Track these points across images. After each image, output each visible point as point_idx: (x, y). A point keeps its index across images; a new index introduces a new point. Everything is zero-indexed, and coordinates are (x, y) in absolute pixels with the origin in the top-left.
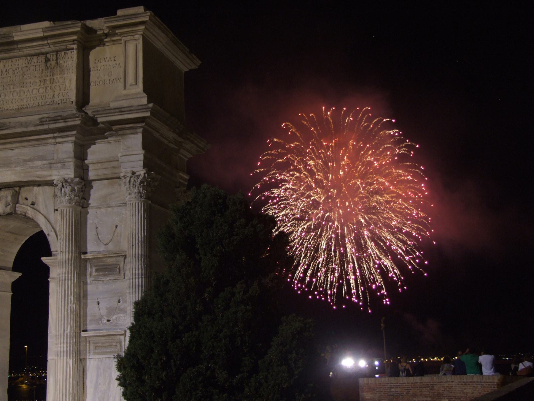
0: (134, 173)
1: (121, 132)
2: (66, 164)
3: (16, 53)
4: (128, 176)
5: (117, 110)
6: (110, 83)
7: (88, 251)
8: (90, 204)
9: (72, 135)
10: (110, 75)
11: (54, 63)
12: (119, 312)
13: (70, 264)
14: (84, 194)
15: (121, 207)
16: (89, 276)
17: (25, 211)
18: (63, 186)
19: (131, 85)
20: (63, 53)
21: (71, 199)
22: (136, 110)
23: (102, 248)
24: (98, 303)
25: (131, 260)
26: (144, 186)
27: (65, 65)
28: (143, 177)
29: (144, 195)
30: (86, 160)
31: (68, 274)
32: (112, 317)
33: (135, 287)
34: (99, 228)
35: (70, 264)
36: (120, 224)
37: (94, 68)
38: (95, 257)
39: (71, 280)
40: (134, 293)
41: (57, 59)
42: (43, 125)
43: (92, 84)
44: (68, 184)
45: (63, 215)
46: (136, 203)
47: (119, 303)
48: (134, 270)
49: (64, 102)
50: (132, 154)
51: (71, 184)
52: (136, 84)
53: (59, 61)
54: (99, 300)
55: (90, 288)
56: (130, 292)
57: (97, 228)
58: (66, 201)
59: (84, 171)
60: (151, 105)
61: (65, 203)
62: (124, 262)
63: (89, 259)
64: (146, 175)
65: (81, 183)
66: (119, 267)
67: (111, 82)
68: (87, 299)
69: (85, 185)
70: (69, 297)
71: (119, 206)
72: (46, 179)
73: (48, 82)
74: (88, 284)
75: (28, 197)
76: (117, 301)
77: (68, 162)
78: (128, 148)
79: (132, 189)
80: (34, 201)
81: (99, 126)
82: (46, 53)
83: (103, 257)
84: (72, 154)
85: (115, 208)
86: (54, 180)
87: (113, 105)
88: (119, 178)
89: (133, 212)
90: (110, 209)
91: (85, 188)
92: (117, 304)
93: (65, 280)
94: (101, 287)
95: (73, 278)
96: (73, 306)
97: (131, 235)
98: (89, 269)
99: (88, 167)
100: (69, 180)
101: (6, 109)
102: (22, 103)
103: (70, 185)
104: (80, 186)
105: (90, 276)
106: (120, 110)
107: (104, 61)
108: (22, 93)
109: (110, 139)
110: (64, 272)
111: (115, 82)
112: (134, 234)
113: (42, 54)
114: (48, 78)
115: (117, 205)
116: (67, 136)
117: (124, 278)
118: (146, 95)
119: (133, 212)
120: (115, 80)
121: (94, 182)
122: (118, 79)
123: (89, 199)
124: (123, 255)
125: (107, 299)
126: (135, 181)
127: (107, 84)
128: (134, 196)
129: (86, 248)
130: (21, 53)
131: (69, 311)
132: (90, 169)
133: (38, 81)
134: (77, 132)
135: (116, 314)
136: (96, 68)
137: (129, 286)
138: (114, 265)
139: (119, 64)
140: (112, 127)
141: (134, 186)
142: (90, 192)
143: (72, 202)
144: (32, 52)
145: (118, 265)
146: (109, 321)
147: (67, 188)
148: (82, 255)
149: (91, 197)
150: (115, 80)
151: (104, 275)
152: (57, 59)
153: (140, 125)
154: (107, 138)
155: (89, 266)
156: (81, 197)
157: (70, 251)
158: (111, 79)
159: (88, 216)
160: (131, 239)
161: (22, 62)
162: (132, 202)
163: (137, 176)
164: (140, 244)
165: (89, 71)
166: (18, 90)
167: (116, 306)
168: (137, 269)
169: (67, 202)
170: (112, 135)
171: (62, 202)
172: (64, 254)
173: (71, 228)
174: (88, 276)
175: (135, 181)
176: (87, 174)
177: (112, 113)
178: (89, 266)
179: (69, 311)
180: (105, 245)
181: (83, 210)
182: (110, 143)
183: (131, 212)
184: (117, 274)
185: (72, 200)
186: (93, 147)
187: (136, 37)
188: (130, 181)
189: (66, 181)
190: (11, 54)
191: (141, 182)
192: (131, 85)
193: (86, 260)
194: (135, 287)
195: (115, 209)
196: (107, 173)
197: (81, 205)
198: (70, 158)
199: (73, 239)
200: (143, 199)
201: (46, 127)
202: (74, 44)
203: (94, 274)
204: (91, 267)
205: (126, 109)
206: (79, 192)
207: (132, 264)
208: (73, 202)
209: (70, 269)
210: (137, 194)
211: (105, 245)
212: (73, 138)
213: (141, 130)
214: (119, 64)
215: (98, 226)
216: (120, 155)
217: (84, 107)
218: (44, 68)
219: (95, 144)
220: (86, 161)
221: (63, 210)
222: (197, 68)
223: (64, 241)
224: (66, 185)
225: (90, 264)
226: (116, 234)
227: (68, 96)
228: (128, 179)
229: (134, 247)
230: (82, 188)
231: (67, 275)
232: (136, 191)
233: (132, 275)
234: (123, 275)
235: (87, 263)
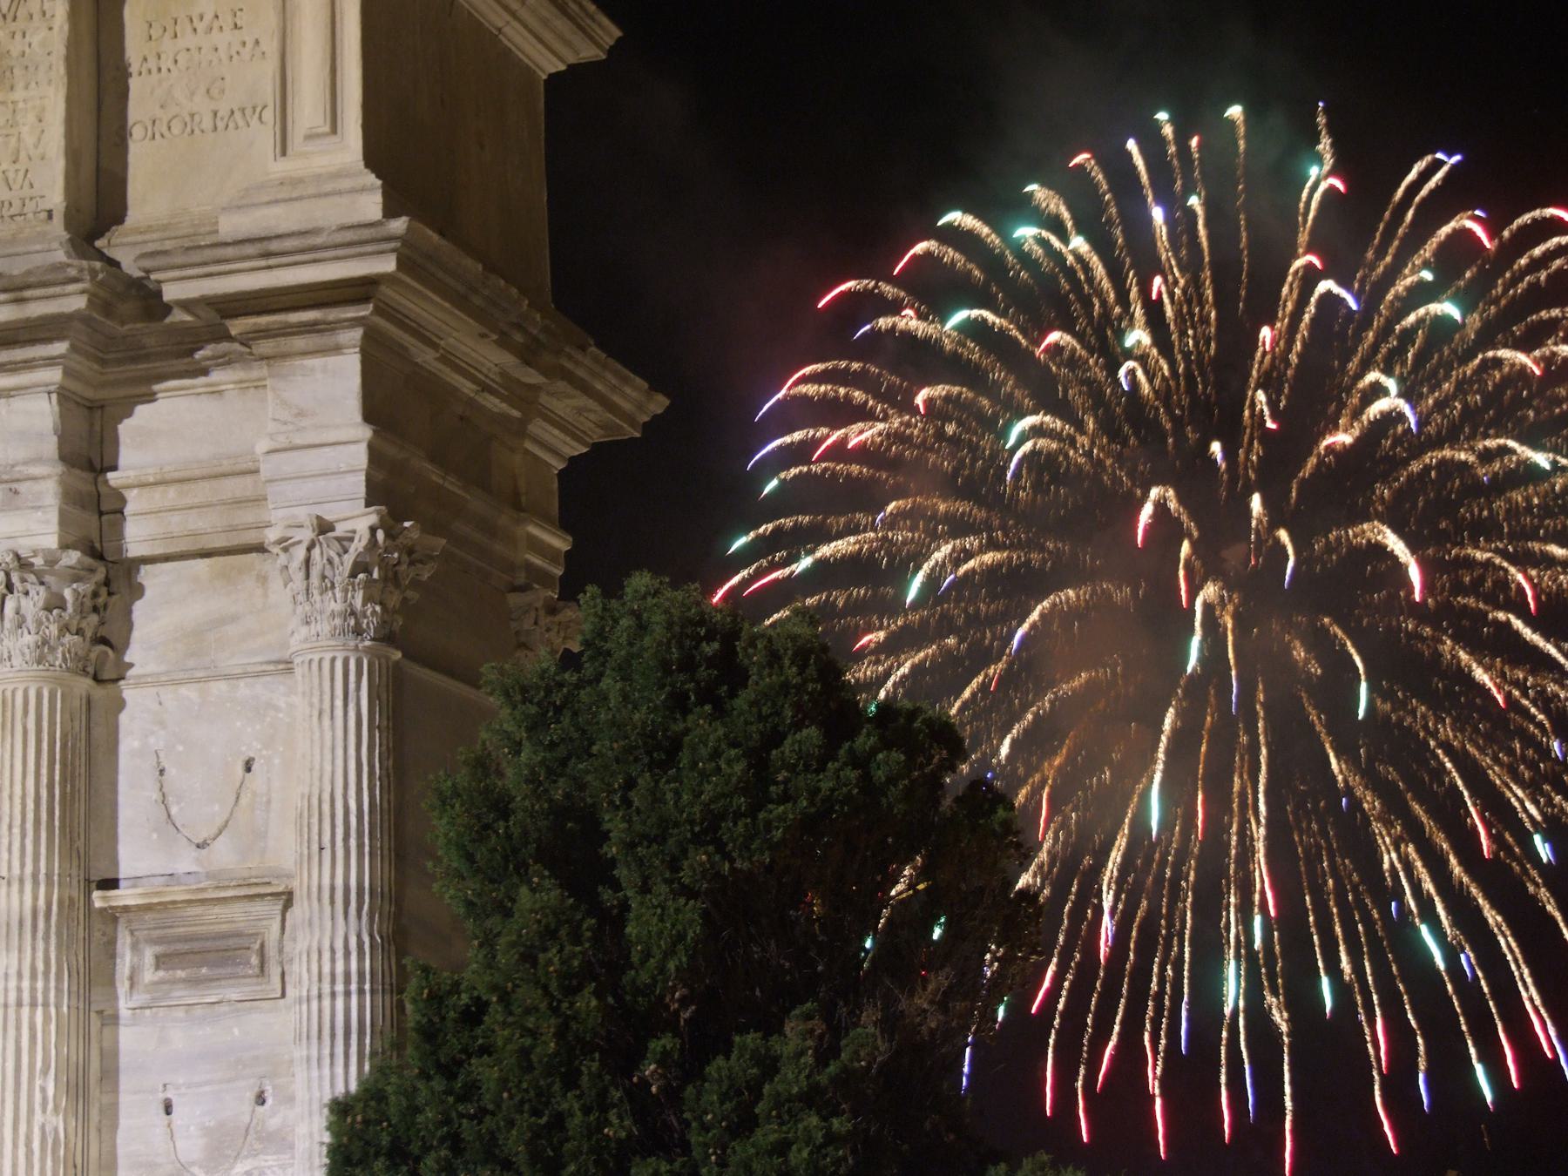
0: (324, 527)
1: (265, 347)
2: (23, 487)
4: (300, 542)
5: (250, 249)
6: (215, 128)
7: (121, 876)
8: (131, 665)
9: (50, 361)
10: (215, 92)
12: (257, 1146)
13: (40, 934)
14: (102, 623)
15: (268, 678)
16: (127, 984)
18: (10, 587)
19: (310, 137)
21: (45, 642)
22: (336, 246)
23: (186, 862)
24: (168, 1109)
25: (311, 912)
26: (369, 584)
27: (15, 53)
28: (364, 541)
29: (370, 623)
30: (114, 468)
31: (34, 977)
32: (232, 1168)
33: (333, 1036)
34: (172, 772)
35: (40, 934)
36: (264, 752)
37: (145, 59)
38: (155, 900)
39: (46, 1005)
40: (327, 1061)
43: (137, 132)
44: (32, 578)
45: (9, 714)
46: (333, 660)
47: (260, 1109)
48: (326, 955)
49: (13, 211)
50: (317, 442)
51: (47, 578)
52: (334, 130)
54: (169, 1095)
55: (130, 1039)
56: (308, 1059)
57: (162, 772)
58: (23, 654)
59: (104, 518)
60: (399, 225)
61: (17, 661)
62: (283, 921)
63: (126, 909)
64: (380, 535)
65: (92, 571)
66: (262, 946)
67: (220, 125)
68: (115, 1090)
69: (107, 582)
70: (38, 1082)
71: (258, 675)
74: (122, 1022)
76: (250, 1095)
77: (34, 479)
78: (301, 414)
79: (317, 597)
81: (168, 320)
83: (189, 902)
84: (51, 446)
85: (242, 683)
87: (232, 225)
88: (260, 549)
89: (321, 701)
90: (220, 687)
91: (110, 594)
92: (253, 1111)
93: (19, 1004)
94: (182, 1036)
95: (57, 996)
96: (54, 1119)
97: (315, 802)
98: (128, 958)
99: (123, 501)
100: (38, 562)
103: (42, 583)
104: (85, 588)
105: (132, 986)
106: (265, 248)
107: (189, 29)
109: (216, 376)
110: (13, 971)
111: (241, 123)
112: (326, 797)
115: (249, 669)
116: (28, 365)
117: (283, 995)
118: (379, 182)
119: (321, 701)
120: (238, 115)
121: (148, 567)
122: (254, 109)
123: (126, 644)
124: (281, 889)
125: (207, 1088)
126: (330, 561)
127: (203, 131)
128: (324, 627)
129: (115, 862)
131: (36, 1145)
132: (127, 511)
134: (73, 348)
135: (246, 1157)
136: (152, 64)
137: (305, 1030)
138: (239, 935)
139: (257, 42)
140: (228, 323)
141: (328, 586)
142: (130, 612)
143: (50, 658)
145: (257, 934)
147: (27, 593)
148: (96, 894)
149: (136, 635)
150: (238, 115)
153: (351, 312)
154: (205, 372)
155: (124, 941)
156: (89, 634)
157: (42, 877)
158: (223, 112)
159: (124, 718)
160: (315, 820)
162: (316, 657)
163: (339, 539)
164: (353, 842)
165: (123, 74)
167: (247, 1119)
168: (340, 954)
169: (28, 658)
170: (226, 361)
171: (6, 656)
172: (15, 887)
173: (44, 771)
174: (122, 988)
175: (330, 561)
176: (120, 535)
177: (227, 261)
178: (128, 940)
179: (36, 1145)
180: (198, 846)
181: (99, 693)
182: (220, 392)
183: (316, 700)
184: (250, 976)
185: (52, 650)
186: (142, 410)
188: (308, 562)
189: (23, 564)
191: (359, 567)
192: (310, 137)
193: (112, 916)
194: (333, 1036)
195: (243, 689)
196: (208, 526)
197: (91, 669)
198: (38, 460)
199: (57, 823)
200: (367, 643)
203: (149, 975)
204: (135, 947)
205: (289, 244)
206: (81, 611)
207: (317, 930)
208: (56, 659)
209: (40, 955)
210: (338, 621)
211: (198, 846)
212: (54, 375)
213: (356, 334)
214: (257, 42)
215: (165, 764)
216: (262, 446)
217: (100, 235)
219: (150, 398)
220: (110, 475)
221: (9, 694)
222: (604, 57)
223: (16, 831)
224: (23, 580)
225: (132, 933)
226: (244, 801)
227: (32, 186)
228: (300, 553)
229: (327, 854)
230: (95, 595)
231: (26, 984)
232: (338, 607)
233: (320, 980)
234: (276, 980)
235: (116, 929)
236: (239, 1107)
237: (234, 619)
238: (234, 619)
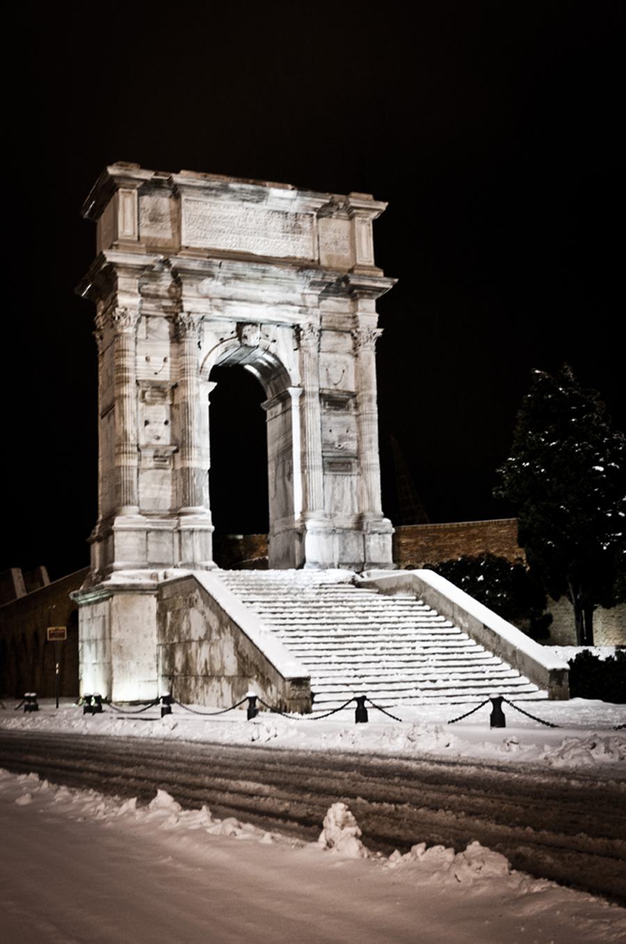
9: (320, 290)
23: (332, 387)
24: (330, 431)
76: (346, 431)
80: (275, 339)
94: (333, 419)
151: (335, 409)
166: (262, 238)
203: (327, 407)
212: (319, 292)
219: (326, 299)
237: (340, 344)
238: (340, 344)
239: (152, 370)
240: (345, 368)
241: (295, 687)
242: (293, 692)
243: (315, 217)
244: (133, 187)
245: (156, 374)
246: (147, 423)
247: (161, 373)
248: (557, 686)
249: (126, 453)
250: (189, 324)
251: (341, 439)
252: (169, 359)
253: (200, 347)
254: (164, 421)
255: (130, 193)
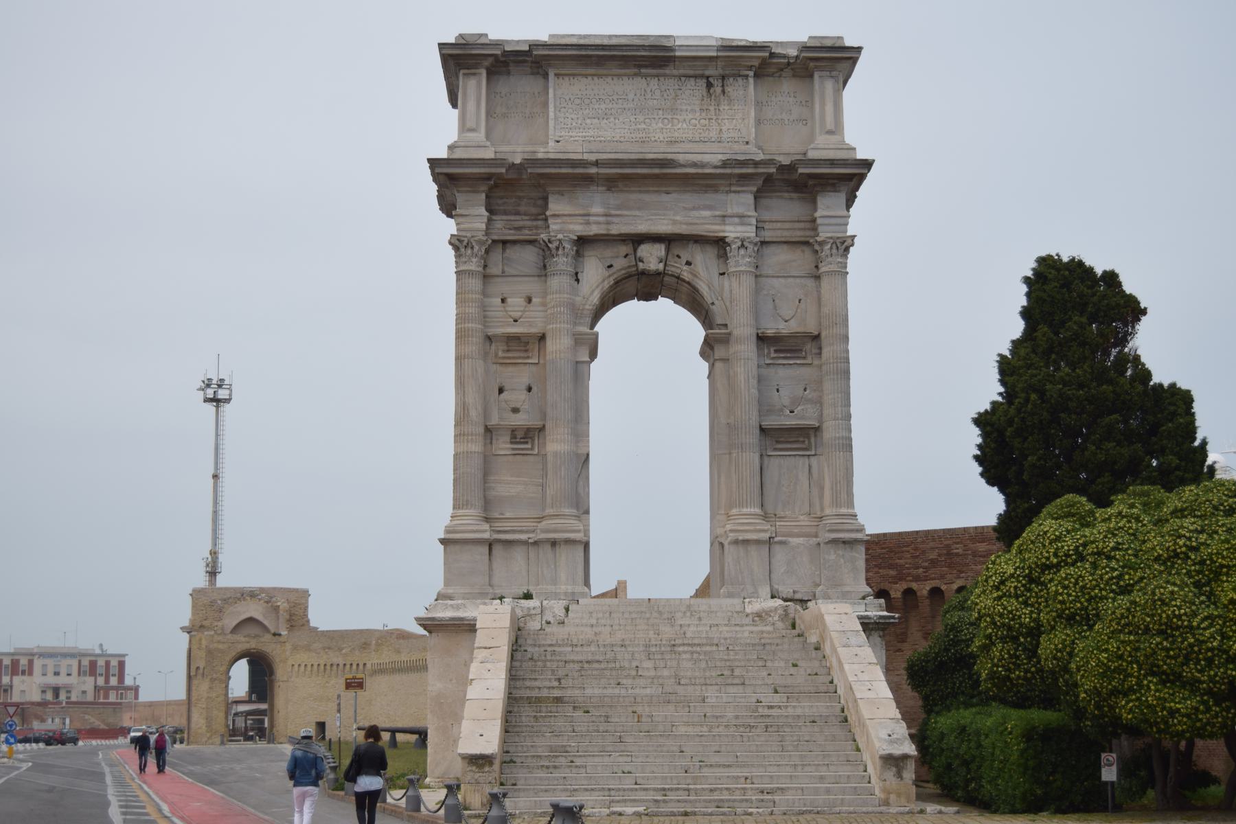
3: (667, 72)
11: (719, 90)
17: (679, 271)
20: (731, 79)
24: (778, 391)
34: (777, 301)
41: (723, 86)
42: (726, 168)
53: (726, 88)
72: (716, 235)
73: (713, 112)
75: (681, 255)
80: (690, 260)
82: (708, 77)
86: (726, 237)
94: (782, 372)
101: (653, 139)
102: (676, 134)
108: (675, 121)
113: (702, 76)
114: (712, 108)
130: (675, 72)
133: (698, 109)
144: (691, 72)
146: (792, 412)
152: (723, 86)
158: (791, 119)
161: (671, 84)
166: (669, 117)
187: (834, 73)
188: (831, 248)
190: (661, 71)
195: (798, 280)
201: (728, 171)
202: (751, 70)
203: (773, 355)
218: (705, 94)
236: (800, 392)
239: (511, 317)
240: (802, 297)
241: (474, 768)
242: (472, 774)
243: (751, 80)
244: (476, 66)
245: (515, 321)
246: (501, 391)
247: (521, 320)
248: (894, 779)
249: (464, 435)
250: (557, 248)
251: (796, 401)
252: (534, 300)
253: (578, 280)
254: (524, 387)
255: (474, 74)
